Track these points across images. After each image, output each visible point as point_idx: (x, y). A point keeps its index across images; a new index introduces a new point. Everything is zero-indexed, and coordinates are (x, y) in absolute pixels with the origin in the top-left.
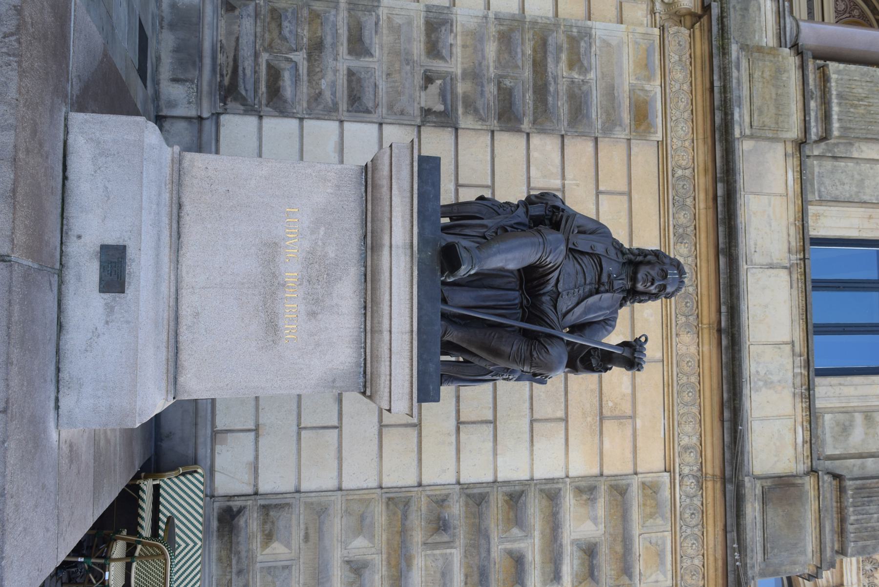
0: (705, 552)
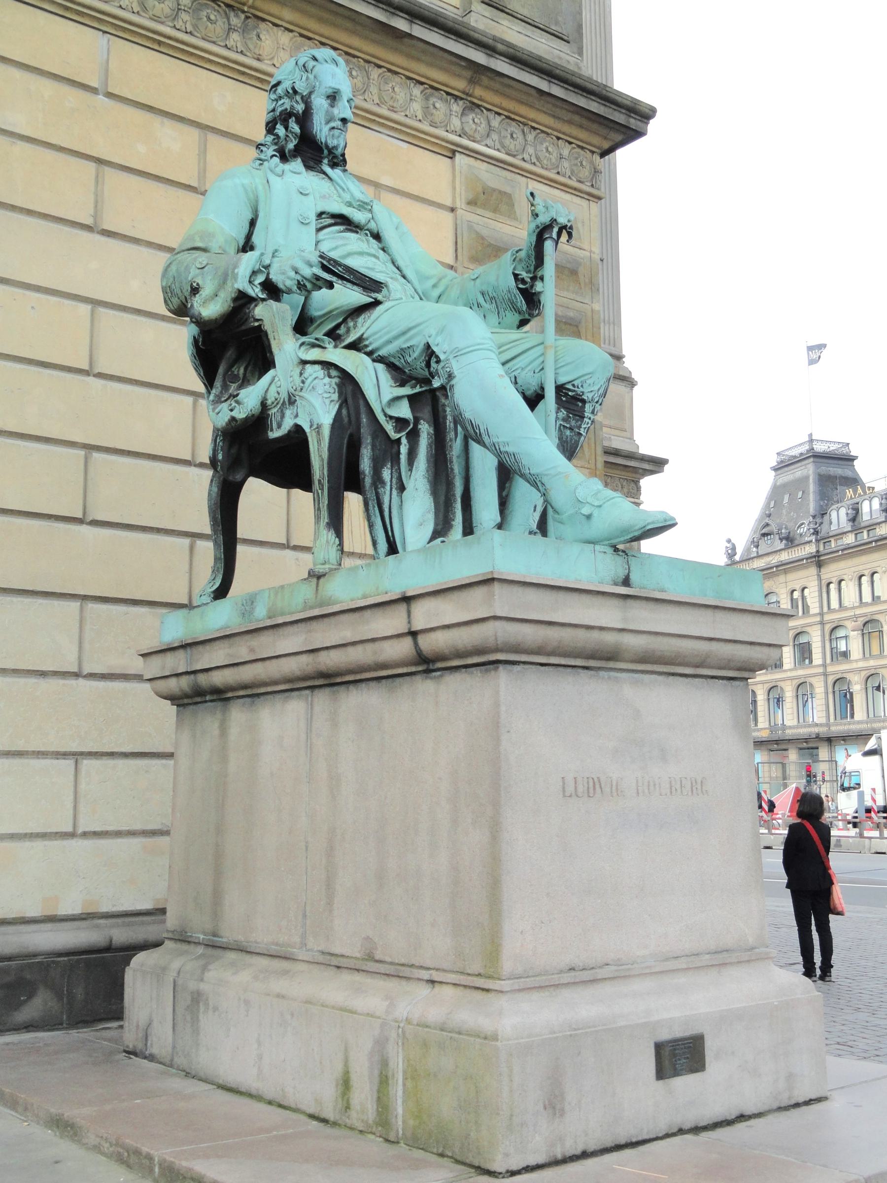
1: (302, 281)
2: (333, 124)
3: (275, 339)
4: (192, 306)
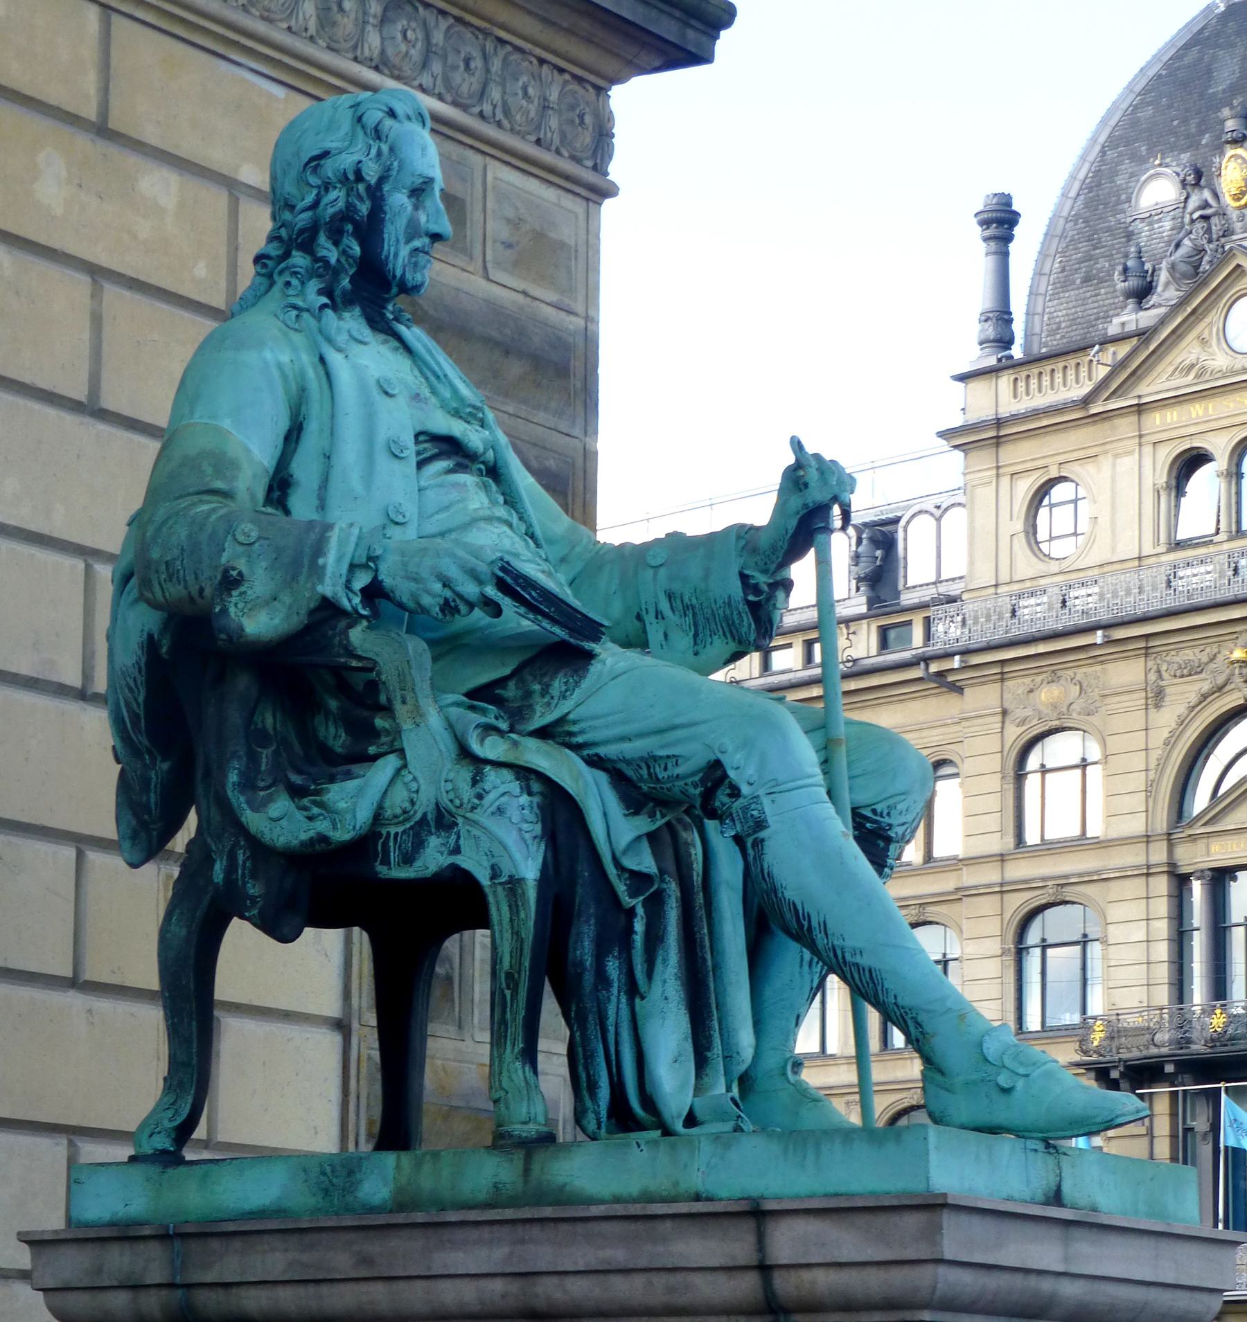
0: (538, 51)
1: (454, 601)
2: (417, 243)
3: (404, 702)
4: (224, 611)
